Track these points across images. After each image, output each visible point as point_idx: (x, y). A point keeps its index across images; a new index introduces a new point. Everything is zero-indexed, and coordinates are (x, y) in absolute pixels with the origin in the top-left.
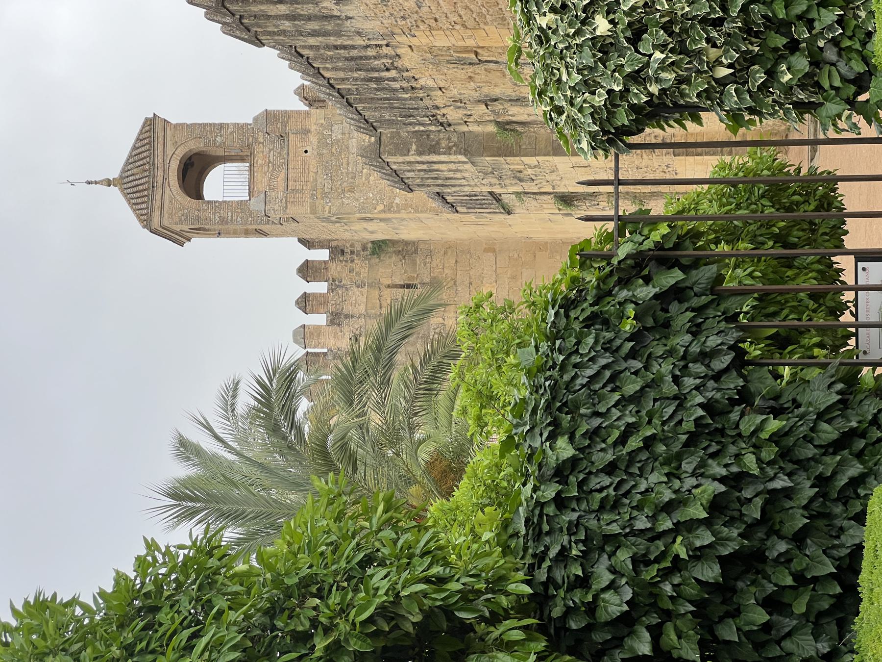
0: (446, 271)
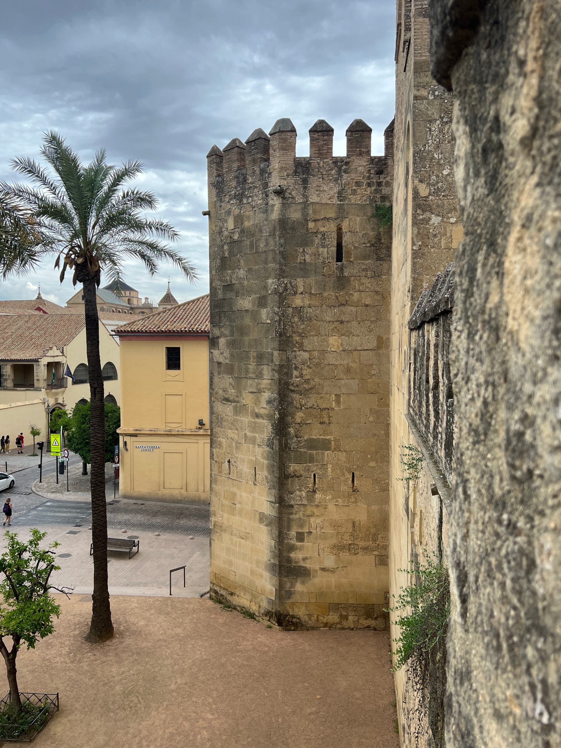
0: (356, 295)
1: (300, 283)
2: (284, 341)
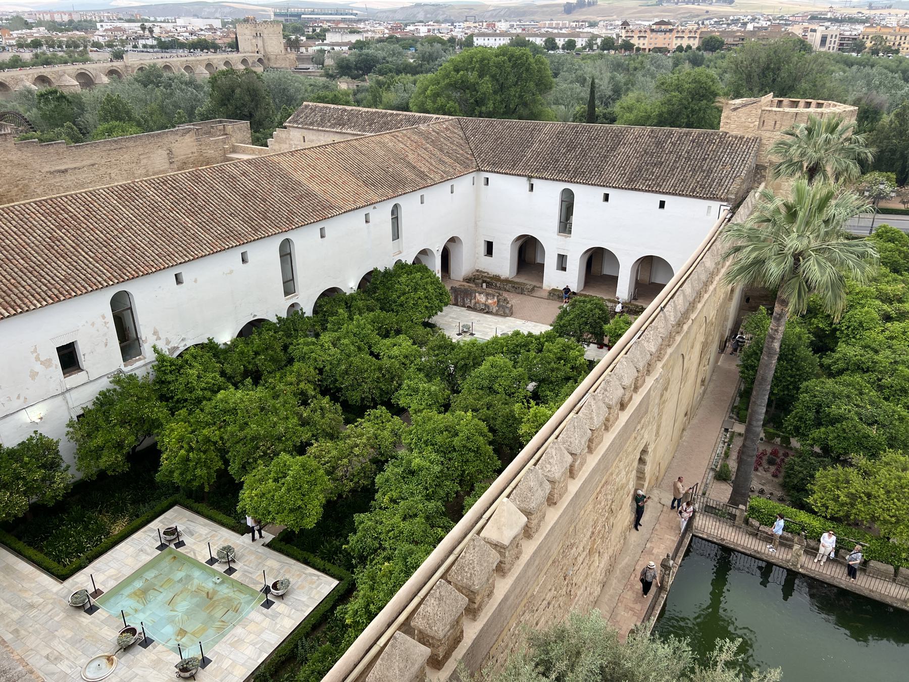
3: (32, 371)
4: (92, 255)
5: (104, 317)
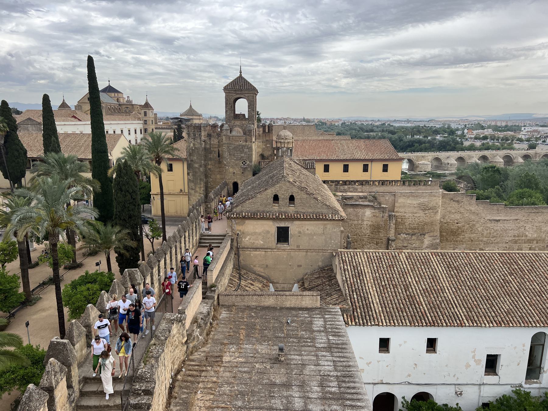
1: (210, 162)
2: (206, 176)
3: (468, 363)
4: (529, 300)
5: (524, 346)
